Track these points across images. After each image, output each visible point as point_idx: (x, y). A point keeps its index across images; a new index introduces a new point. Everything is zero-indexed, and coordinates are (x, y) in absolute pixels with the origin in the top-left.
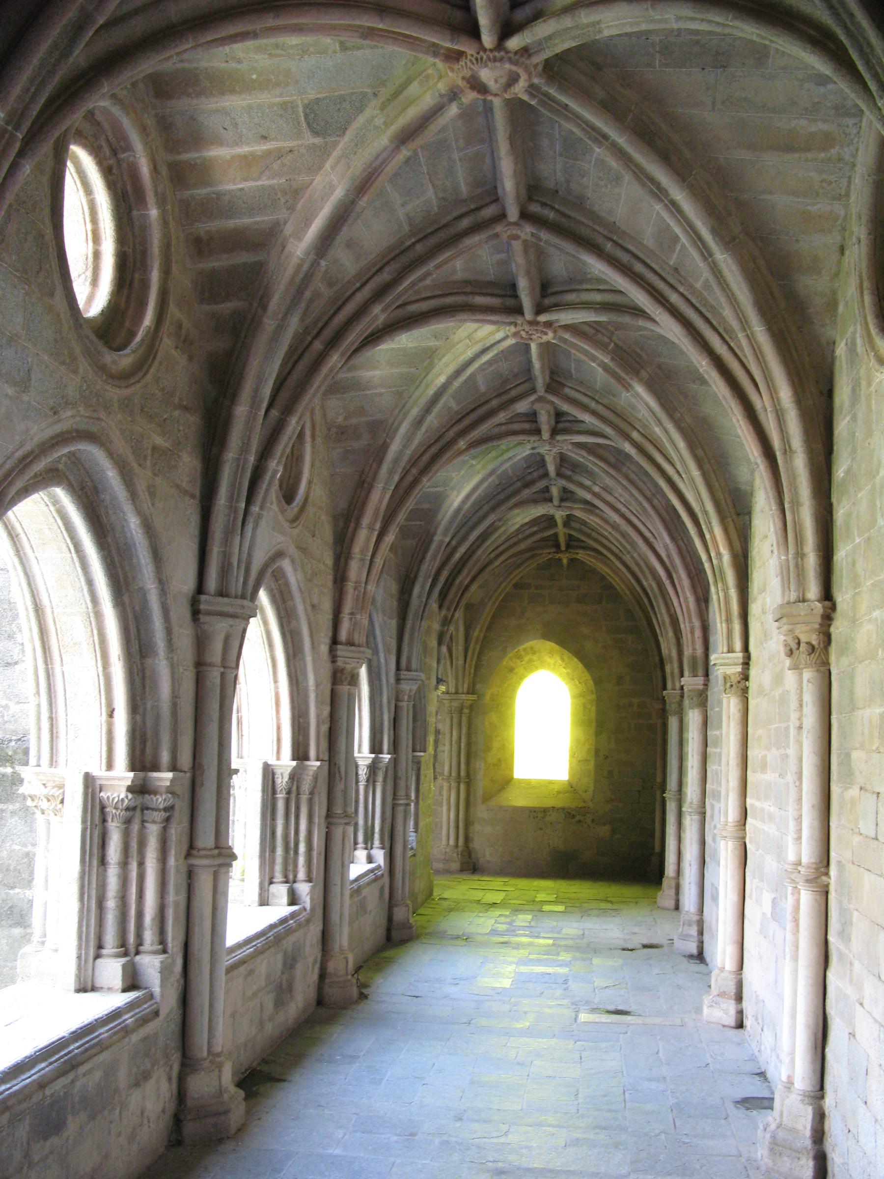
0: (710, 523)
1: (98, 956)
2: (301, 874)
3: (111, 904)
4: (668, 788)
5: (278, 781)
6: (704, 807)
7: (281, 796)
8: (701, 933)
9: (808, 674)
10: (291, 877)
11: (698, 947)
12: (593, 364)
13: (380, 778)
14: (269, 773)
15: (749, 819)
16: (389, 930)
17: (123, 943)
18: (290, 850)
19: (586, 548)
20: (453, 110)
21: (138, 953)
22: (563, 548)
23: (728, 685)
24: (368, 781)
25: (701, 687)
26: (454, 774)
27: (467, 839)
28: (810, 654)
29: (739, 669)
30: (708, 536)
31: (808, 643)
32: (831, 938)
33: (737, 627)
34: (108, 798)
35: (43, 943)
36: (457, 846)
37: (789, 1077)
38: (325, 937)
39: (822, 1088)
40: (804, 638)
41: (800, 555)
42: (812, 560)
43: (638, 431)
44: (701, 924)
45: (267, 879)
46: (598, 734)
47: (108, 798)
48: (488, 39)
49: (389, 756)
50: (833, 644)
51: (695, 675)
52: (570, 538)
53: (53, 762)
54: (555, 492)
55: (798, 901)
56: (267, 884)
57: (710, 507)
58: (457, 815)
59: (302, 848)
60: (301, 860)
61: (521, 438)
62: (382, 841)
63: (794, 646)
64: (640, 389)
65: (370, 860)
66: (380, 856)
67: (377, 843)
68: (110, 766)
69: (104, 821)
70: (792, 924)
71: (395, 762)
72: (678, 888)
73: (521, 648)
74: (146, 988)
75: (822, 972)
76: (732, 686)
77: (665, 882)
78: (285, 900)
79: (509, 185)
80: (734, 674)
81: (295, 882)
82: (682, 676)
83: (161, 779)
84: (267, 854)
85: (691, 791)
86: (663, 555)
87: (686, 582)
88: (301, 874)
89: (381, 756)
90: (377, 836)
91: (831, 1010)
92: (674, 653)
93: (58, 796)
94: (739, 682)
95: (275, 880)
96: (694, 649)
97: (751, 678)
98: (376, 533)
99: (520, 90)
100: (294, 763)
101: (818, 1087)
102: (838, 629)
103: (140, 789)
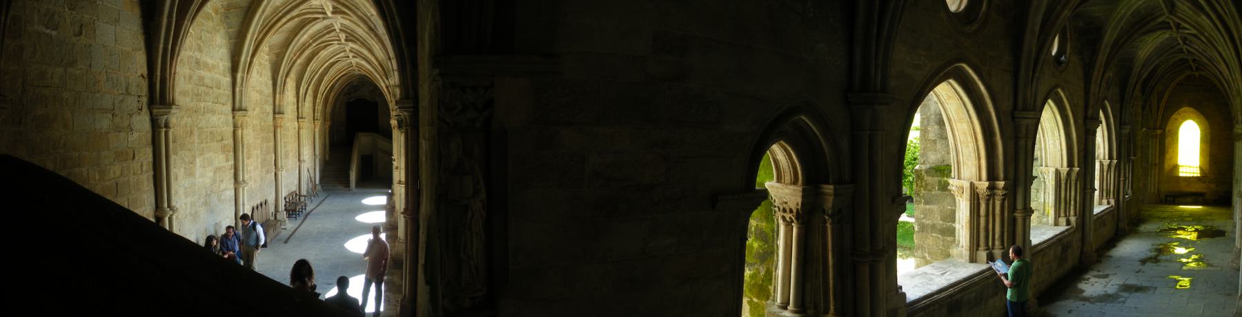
2: (1072, 213)
5: (1062, 176)
7: (1063, 183)
10: (1068, 214)
13: (1113, 170)
14: (1057, 173)
24: (1108, 171)
46: (1211, 146)
59: (1072, 203)
60: (1072, 208)
61: (1164, 31)
62: (1114, 195)
66: (1112, 202)
67: (1111, 196)
78: (1065, 224)
88: (1072, 213)
90: (1112, 194)
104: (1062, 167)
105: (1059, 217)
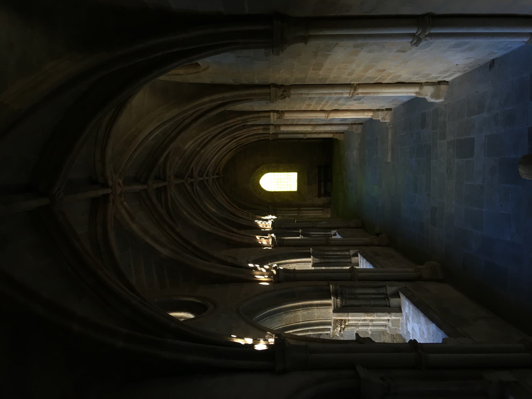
0: (228, 124)
1: (389, 306)
2: (347, 253)
3: (373, 303)
4: (303, 137)
6: (313, 124)
8: (355, 124)
9: (292, 92)
10: (348, 256)
11: (360, 125)
12: (179, 163)
15: (324, 109)
16: (358, 228)
17: (384, 299)
19: (219, 169)
20: (125, 203)
23: (281, 117)
25: (273, 127)
26: (297, 212)
27: (319, 206)
28: (286, 91)
29: (276, 114)
30: (232, 125)
31: (283, 92)
32: (373, 83)
33: (262, 115)
35: (386, 326)
36: (322, 210)
37: (415, 93)
38: (366, 245)
39: (418, 83)
40: (281, 93)
41: (255, 95)
42: (257, 91)
43: (197, 148)
44: (352, 124)
45: (350, 264)
48: (109, 191)
49: (300, 230)
50: (283, 84)
51: (269, 129)
52: (217, 174)
53: (329, 324)
54: (206, 178)
55: (361, 93)
57: (223, 124)
58: (311, 210)
59: (339, 253)
62: (329, 231)
63: (283, 96)
64: (187, 147)
65: (335, 235)
66: (333, 232)
67: (329, 233)
69: (347, 306)
70: (368, 94)
71: (301, 228)
72: (337, 133)
73: (252, 190)
75: (383, 84)
76: (281, 116)
77: (335, 137)
78: (356, 258)
79: (138, 187)
80: (277, 115)
82: (269, 134)
83: (333, 289)
85: (309, 129)
86: (229, 140)
87: (238, 132)
88: (347, 253)
90: (327, 233)
91: (395, 81)
92: (257, 137)
93: (340, 321)
94: (280, 114)
96: (261, 129)
97: (278, 110)
98: (234, 234)
99: (121, 181)
100: (312, 257)
101: (418, 84)
102: (280, 83)
104: (310, 262)
105: (351, 263)
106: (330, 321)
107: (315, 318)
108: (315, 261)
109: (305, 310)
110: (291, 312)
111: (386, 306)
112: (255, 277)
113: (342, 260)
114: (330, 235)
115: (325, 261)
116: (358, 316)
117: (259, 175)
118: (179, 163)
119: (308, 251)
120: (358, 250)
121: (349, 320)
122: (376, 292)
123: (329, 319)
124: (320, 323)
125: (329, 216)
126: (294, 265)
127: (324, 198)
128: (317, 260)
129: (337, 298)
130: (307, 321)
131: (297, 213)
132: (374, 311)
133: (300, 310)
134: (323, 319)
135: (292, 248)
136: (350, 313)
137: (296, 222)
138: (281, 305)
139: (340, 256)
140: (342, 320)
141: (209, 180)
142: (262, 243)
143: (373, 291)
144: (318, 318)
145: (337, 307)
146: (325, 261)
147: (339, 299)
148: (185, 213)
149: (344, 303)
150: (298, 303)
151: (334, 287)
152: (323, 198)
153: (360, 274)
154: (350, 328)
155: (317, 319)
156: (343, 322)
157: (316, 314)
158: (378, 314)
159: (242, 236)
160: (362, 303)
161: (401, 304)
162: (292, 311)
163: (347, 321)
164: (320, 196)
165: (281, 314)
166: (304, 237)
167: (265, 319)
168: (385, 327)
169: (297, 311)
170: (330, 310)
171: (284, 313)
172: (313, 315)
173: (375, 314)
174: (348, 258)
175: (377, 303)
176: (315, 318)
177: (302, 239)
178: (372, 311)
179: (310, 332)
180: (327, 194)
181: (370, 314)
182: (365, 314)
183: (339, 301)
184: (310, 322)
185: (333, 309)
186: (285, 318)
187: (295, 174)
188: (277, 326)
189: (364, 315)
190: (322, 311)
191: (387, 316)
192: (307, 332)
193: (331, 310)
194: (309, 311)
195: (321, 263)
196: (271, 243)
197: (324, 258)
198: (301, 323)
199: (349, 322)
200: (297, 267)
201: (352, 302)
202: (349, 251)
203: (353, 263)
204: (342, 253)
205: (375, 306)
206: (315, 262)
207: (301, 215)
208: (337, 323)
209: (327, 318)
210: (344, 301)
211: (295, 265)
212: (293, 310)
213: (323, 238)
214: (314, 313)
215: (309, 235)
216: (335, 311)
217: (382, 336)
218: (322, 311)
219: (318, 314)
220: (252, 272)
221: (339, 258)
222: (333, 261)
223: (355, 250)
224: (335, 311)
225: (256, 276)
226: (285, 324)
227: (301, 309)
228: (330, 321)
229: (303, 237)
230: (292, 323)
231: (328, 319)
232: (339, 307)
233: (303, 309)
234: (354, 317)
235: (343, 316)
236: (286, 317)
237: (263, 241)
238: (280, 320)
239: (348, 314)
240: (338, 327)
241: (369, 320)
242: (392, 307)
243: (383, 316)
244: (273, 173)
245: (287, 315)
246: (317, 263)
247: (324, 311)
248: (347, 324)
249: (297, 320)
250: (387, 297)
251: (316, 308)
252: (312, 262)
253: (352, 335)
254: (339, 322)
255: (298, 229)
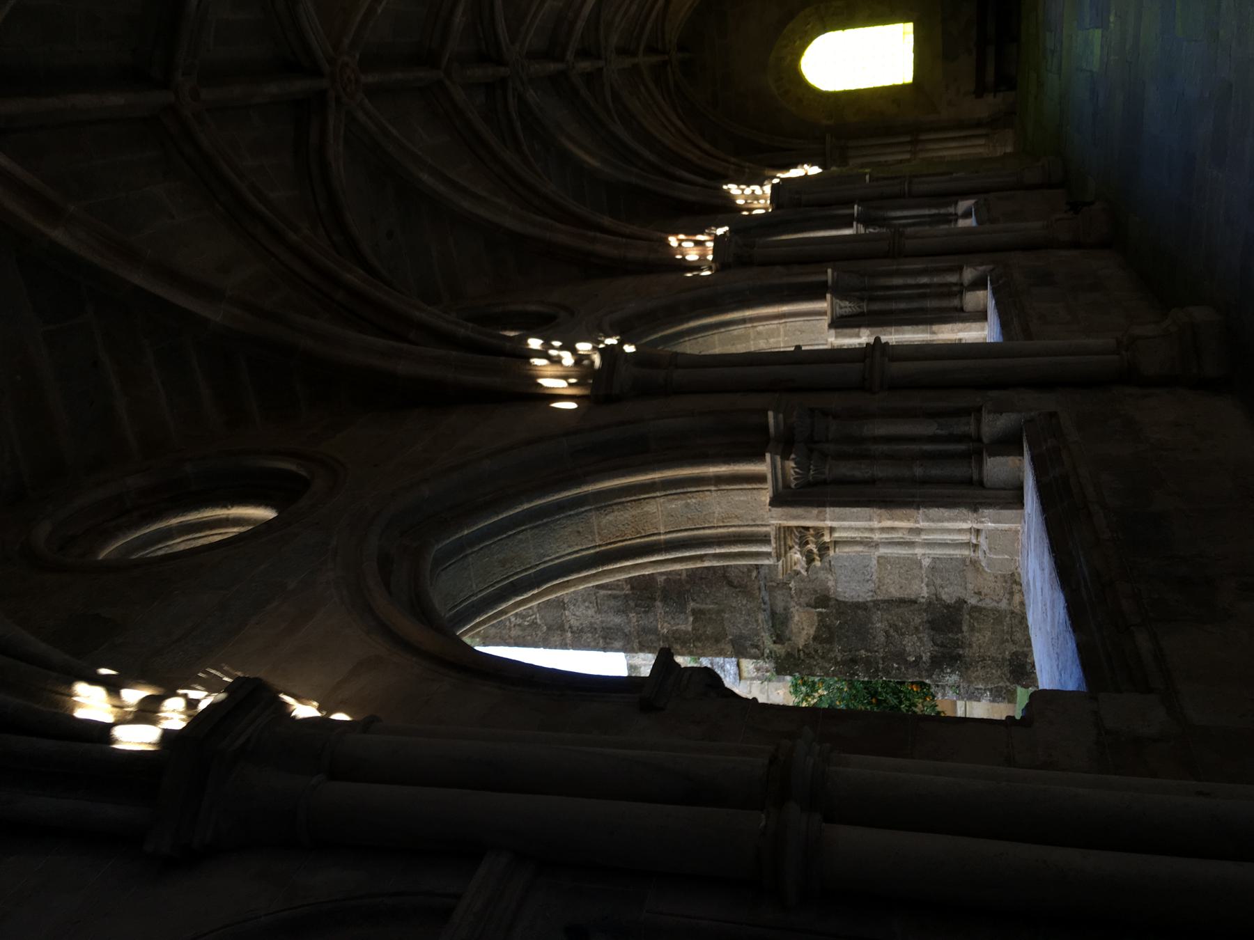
1: (981, 484)
2: (953, 278)
3: (918, 471)
10: (955, 289)
17: (965, 456)
18: (925, 292)
21: (979, 440)
22: (667, 57)
26: (909, 148)
27: (979, 124)
34: (795, 479)
36: (986, 136)
38: (1030, 246)
45: (957, 314)
47: (795, 479)
49: (856, 207)
52: (651, 50)
53: (765, 540)
56: (963, 314)
58: (953, 139)
59: (925, 280)
62: (948, 205)
67: (951, 210)
68: (759, 479)
69: (825, 483)
71: (861, 201)
74: (1021, 429)
81: (962, 284)
84: (929, 316)
88: (953, 278)
89: (856, 215)
90: (943, 211)
93: (800, 532)
95: (959, 306)
98: (598, 235)
103: (786, 445)
106: (767, 529)
107: (713, 522)
108: (841, 308)
109: (676, 497)
110: (623, 503)
111: (969, 482)
112: (541, 385)
113: (929, 304)
114: (951, 218)
115: (876, 306)
116: (857, 519)
117: (795, 42)
118: (379, 11)
119: (821, 278)
120: (991, 267)
121: (832, 530)
122: (939, 432)
123: (762, 525)
124: (734, 536)
125: (1009, 149)
126: (771, 326)
127: (995, 96)
128: (847, 307)
129: (785, 457)
130: (686, 530)
131: (908, 152)
132: (918, 499)
133: (657, 497)
134: (740, 523)
135: (779, 268)
136: (828, 510)
137: (870, 181)
138: (579, 485)
139: (928, 290)
140: (807, 528)
141: (605, 70)
142: (684, 259)
143: (930, 428)
144: (723, 522)
145: (786, 486)
146: (876, 306)
147: (793, 459)
148: (425, 177)
149: (812, 472)
150: (647, 474)
151: (781, 416)
152: (990, 98)
153: (896, 368)
154: (847, 549)
155: (721, 524)
156: (812, 535)
157: (717, 510)
158: (931, 511)
159: (624, 240)
160: (879, 471)
161: (1023, 477)
162: (624, 500)
163: (827, 533)
164: (980, 90)
165: (583, 512)
166: (866, 227)
167: (510, 533)
168: (972, 549)
169: (645, 499)
170: (765, 496)
171: (593, 507)
172: (704, 513)
173: (921, 511)
174: (951, 295)
175: (936, 471)
176: (713, 522)
177: (861, 235)
178: (910, 499)
179: (710, 561)
180: (1006, 81)
181: (899, 512)
182: (883, 511)
183: (793, 468)
184: (696, 532)
185: (772, 495)
186: (599, 525)
187: (909, 27)
188: (570, 550)
189: (880, 516)
190: (737, 499)
191: (964, 521)
192: (699, 562)
193: (766, 496)
194: (690, 498)
195: (861, 314)
196: (710, 257)
197: (872, 299)
198: (662, 537)
199: (836, 535)
200: (782, 330)
201: (845, 469)
202: (960, 269)
203: (968, 312)
204: (936, 280)
205: (924, 482)
206: (838, 311)
207: (922, 155)
208: (789, 538)
209: (754, 520)
210: (812, 467)
211: (774, 326)
212: (629, 499)
213: (927, 228)
214: (708, 504)
215: (885, 219)
216: (777, 501)
217: (970, 575)
218: (737, 499)
219: (722, 508)
220: (528, 367)
221: (923, 296)
222: (903, 306)
223: (981, 268)
224: (777, 501)
225: (541, 381)
226: (601, 543)
227: (658, 494)
228: (767, 529)
229: (862, 230)
230: (630, 539)
231: (758, 526)
232: (793, 486)
233: (668, 492)
234: (844, 520)
235: (804, 518)
236: (604, 521)
237: (689, 252)
238: (579, 532)
239: (820, 512)
240: (793, 550)
241: (907, 528)
242: (990, 489)
243: (949, 520)
244: (841, 31)
245: (606, 515)
246: (846, 316)
247: (742, 499)
248: (827, 538)
249: (646, 528)
250: (977, 450)
251: (713, 488)
252: (829, 313)
253: (865, 567)
254: (796, 536)
255: (849, 203)
